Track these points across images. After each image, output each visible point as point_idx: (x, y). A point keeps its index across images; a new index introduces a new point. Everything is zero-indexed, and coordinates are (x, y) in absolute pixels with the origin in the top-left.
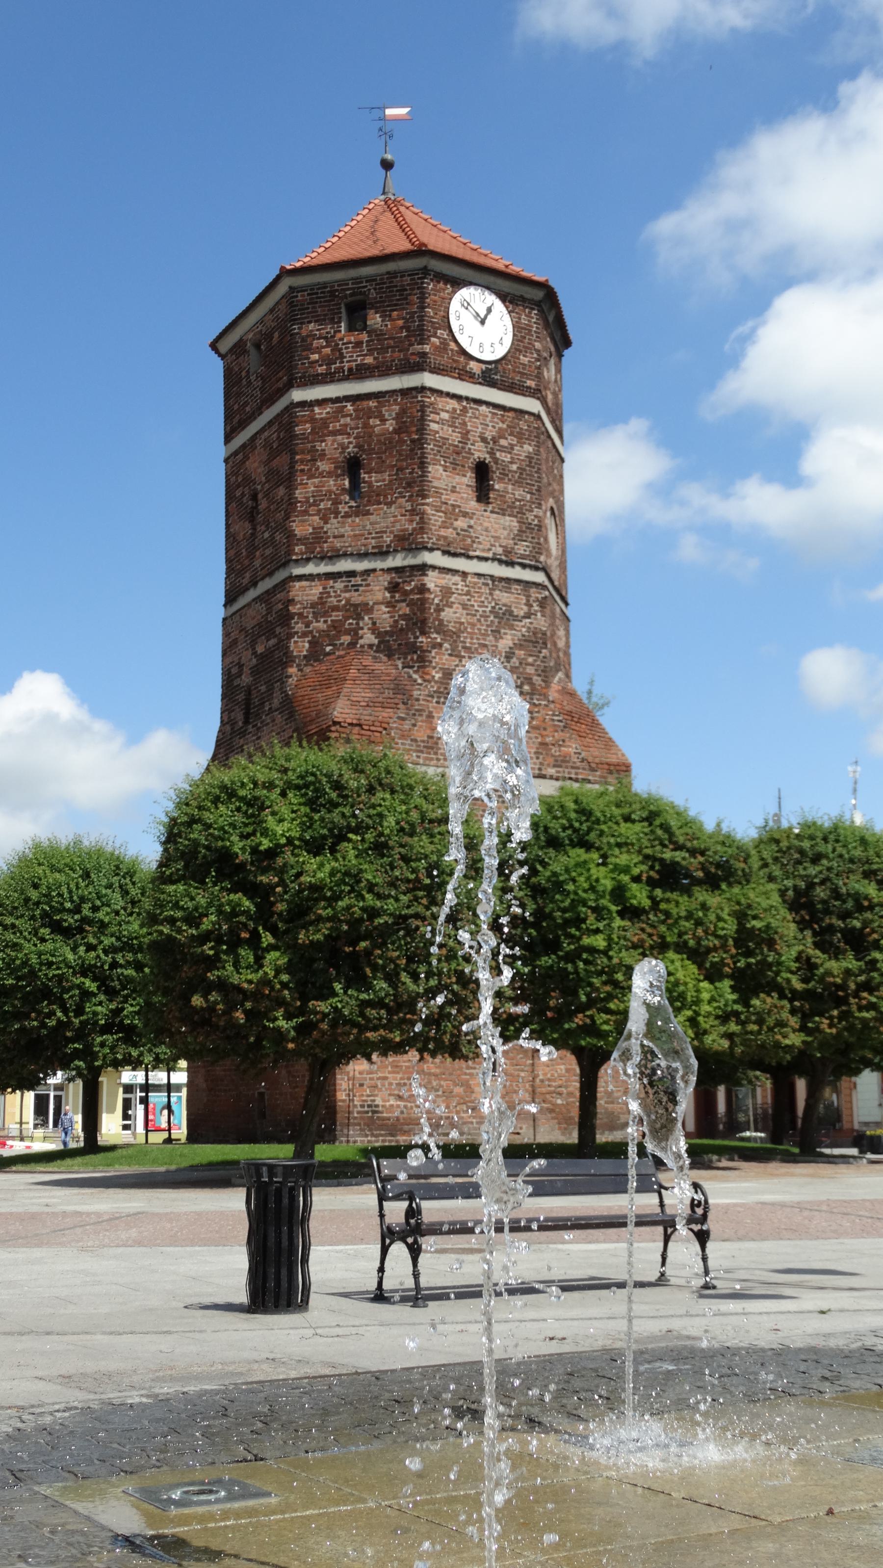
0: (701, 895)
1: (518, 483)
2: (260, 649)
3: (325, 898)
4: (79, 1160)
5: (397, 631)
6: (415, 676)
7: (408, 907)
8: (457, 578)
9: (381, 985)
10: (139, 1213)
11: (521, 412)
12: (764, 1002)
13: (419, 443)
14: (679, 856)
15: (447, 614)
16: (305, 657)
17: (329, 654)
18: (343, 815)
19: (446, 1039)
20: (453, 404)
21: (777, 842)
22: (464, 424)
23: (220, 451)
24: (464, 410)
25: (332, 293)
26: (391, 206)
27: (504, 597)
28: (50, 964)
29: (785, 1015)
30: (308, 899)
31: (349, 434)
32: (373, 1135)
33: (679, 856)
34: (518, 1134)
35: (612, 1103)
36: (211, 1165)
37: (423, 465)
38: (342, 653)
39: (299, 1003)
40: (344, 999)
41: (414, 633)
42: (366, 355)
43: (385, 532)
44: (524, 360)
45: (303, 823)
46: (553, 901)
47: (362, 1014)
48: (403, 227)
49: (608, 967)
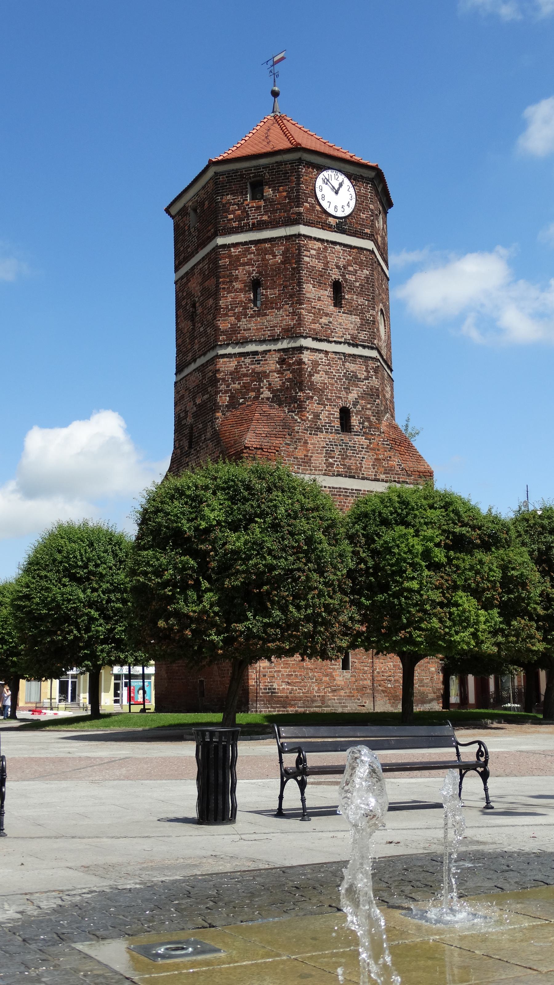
0: (479, 555)
1: (359, 294)
2: (198, 401)
3: (241, 559)
4: (88, 723)
5: (284, 389)
6: (296, 417)
7: (294, 564)
8: (322, 355)
9: (277, 613)
10: (127, 758)
11: (361, 249)
12: (520, 623)
13: (297, 270)
14: (464, 530)
15: (316, 378)
16: (227, 406)
17: (242, 404)
18: (252, 506)
19: (318, 647)
20: (318, 245)
21: (527, 520)
22: (326, 257)
23: (172, 277)
24: (326, 248)
25: (241, 176)
26: (278, 120)
27: (352, 367)
28: (69, 601)
29: (533, 631)
30: (231, 559)
31: (253, 265)
32: (272, 707)
33: (464, 530)
34: (364, 706)
35: (423, 686)
36: (171, 726)
37: (300, 284)
38: (250, 403)
39: (225, 625)
40: (253, 622)
41: (295, 391)
42: (263, 215)
43: (276, 326)
44: (363, 216)
45: (227, 511)
46: (385, 559)
47: (265, 632)
48: (286, 133)
49: (420, 601)
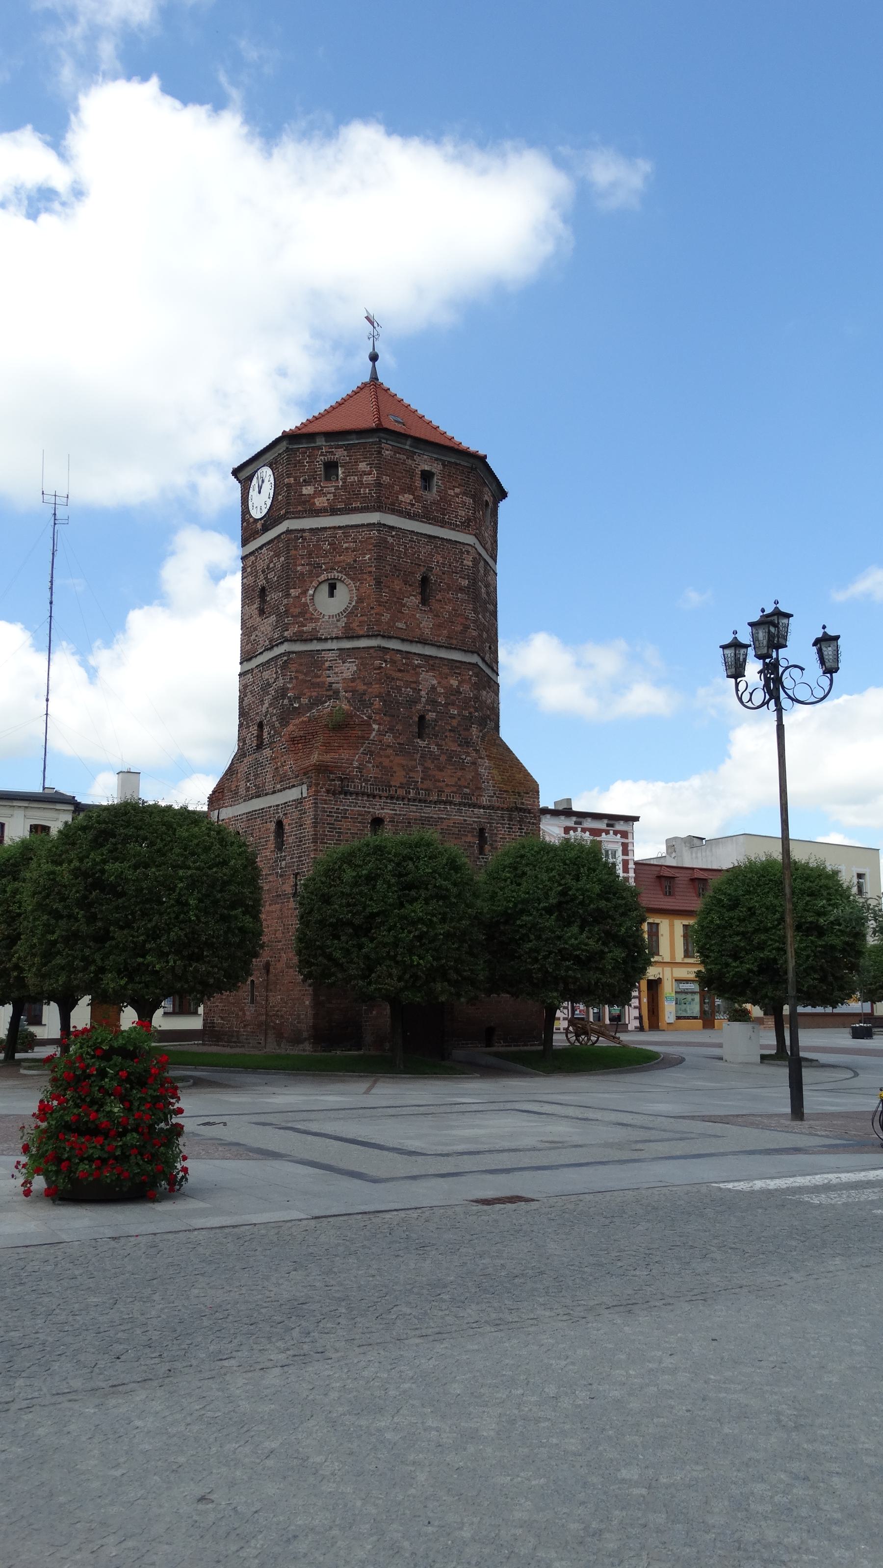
20: (252, 558)
27: (266, 675)
